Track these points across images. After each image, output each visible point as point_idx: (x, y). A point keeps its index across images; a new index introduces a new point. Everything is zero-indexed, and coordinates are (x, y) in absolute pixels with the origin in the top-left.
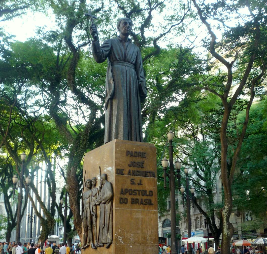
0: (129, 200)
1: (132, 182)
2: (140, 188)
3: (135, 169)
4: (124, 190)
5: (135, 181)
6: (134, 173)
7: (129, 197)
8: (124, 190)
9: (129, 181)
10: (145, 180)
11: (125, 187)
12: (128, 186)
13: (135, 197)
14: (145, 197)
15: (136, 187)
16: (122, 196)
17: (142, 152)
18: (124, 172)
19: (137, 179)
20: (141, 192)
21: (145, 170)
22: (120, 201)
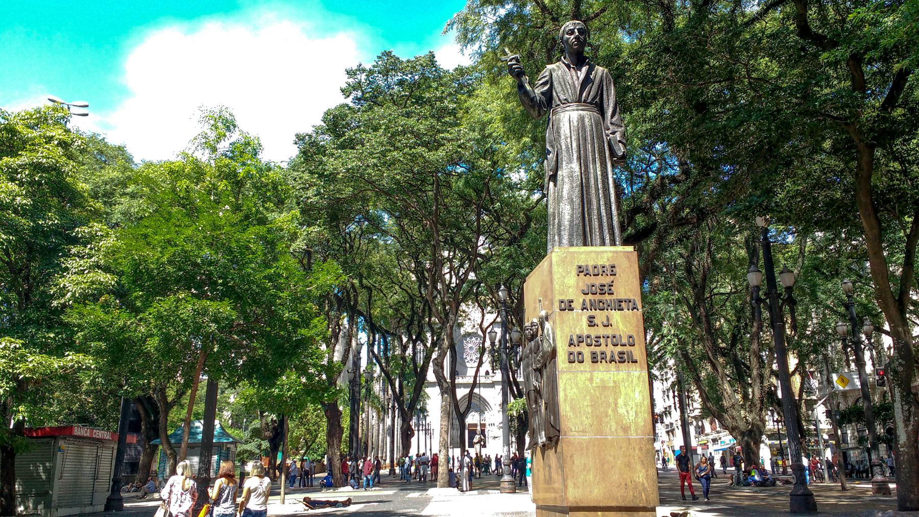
1: (591, 322)
2: (609, 332)
3: (598, 297)
4: (575, 338)
5: (596, 321)
6: (593, 306)
7: (586, 351)
8: (575, 338)
9: (584, 321)
10: (616, 316)
11: (578, 332)
13: (598, 350)
14: (619, 349)
15: (601, 331)
16: (575, 350)
17: (607, 264)
18: (573, 305)
20: (609, 340)
21: (614, 297)
22: (569, 358)
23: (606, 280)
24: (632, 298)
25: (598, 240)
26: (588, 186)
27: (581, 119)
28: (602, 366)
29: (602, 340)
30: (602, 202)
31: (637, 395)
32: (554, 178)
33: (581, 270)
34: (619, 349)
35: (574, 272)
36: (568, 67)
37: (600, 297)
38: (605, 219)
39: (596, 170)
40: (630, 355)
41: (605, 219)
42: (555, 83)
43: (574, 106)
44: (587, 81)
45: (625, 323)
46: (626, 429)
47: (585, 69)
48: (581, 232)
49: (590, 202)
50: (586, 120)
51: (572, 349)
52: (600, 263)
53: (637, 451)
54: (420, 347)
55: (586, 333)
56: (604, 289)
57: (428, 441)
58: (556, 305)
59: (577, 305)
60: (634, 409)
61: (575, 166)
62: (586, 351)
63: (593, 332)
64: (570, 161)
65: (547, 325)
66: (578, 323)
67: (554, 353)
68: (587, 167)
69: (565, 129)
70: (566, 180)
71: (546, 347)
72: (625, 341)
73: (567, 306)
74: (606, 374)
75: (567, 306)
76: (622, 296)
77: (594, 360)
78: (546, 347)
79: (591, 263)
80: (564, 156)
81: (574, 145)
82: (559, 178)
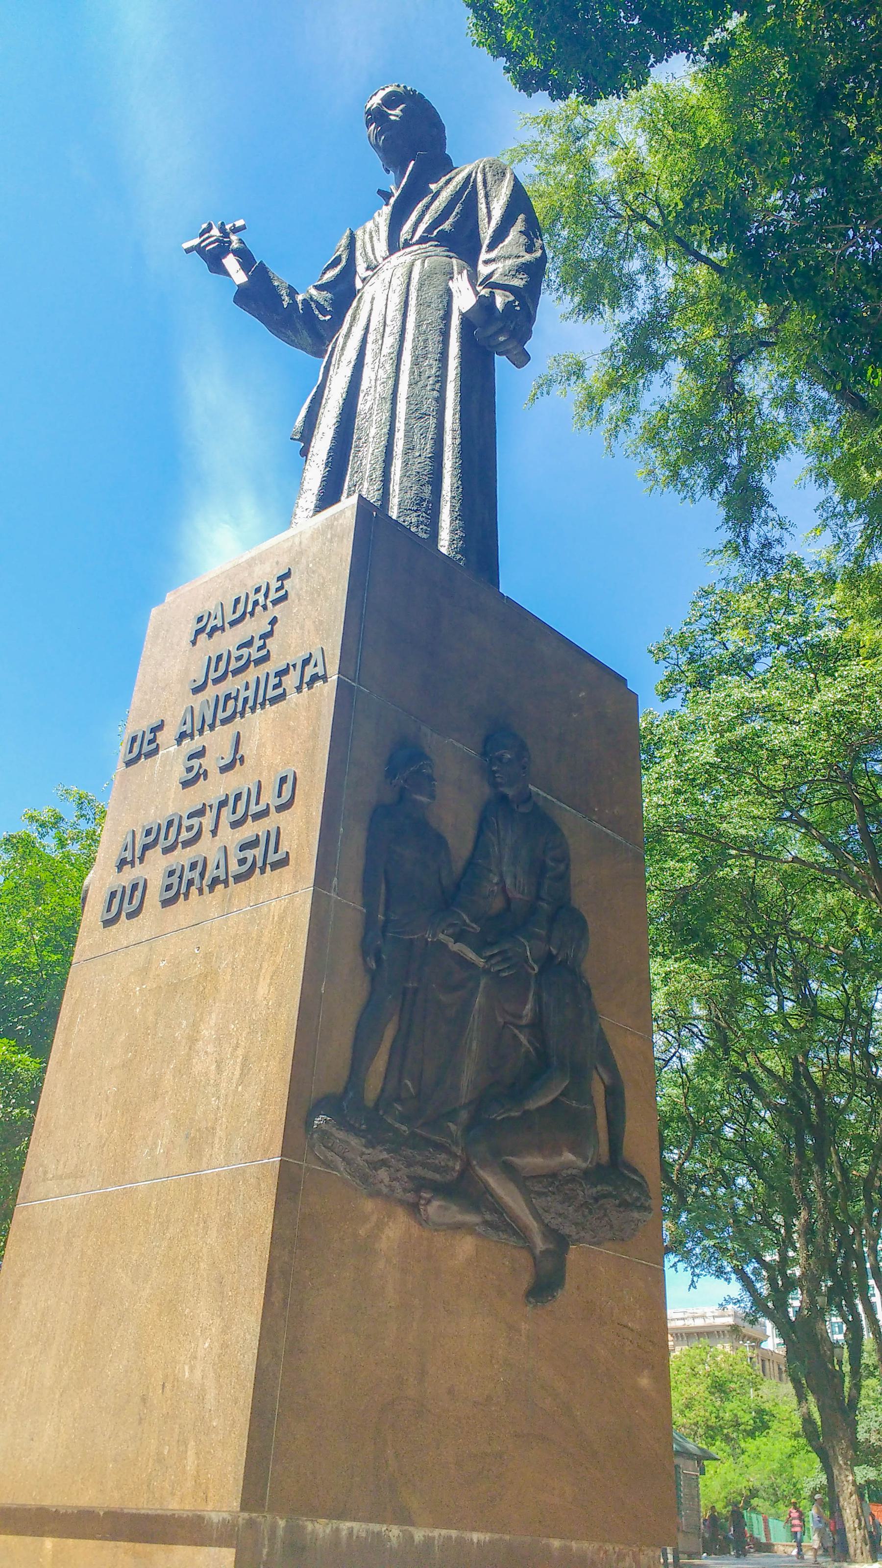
31: (262, 989)
53: (214, 1233)
60: (240, 1052)
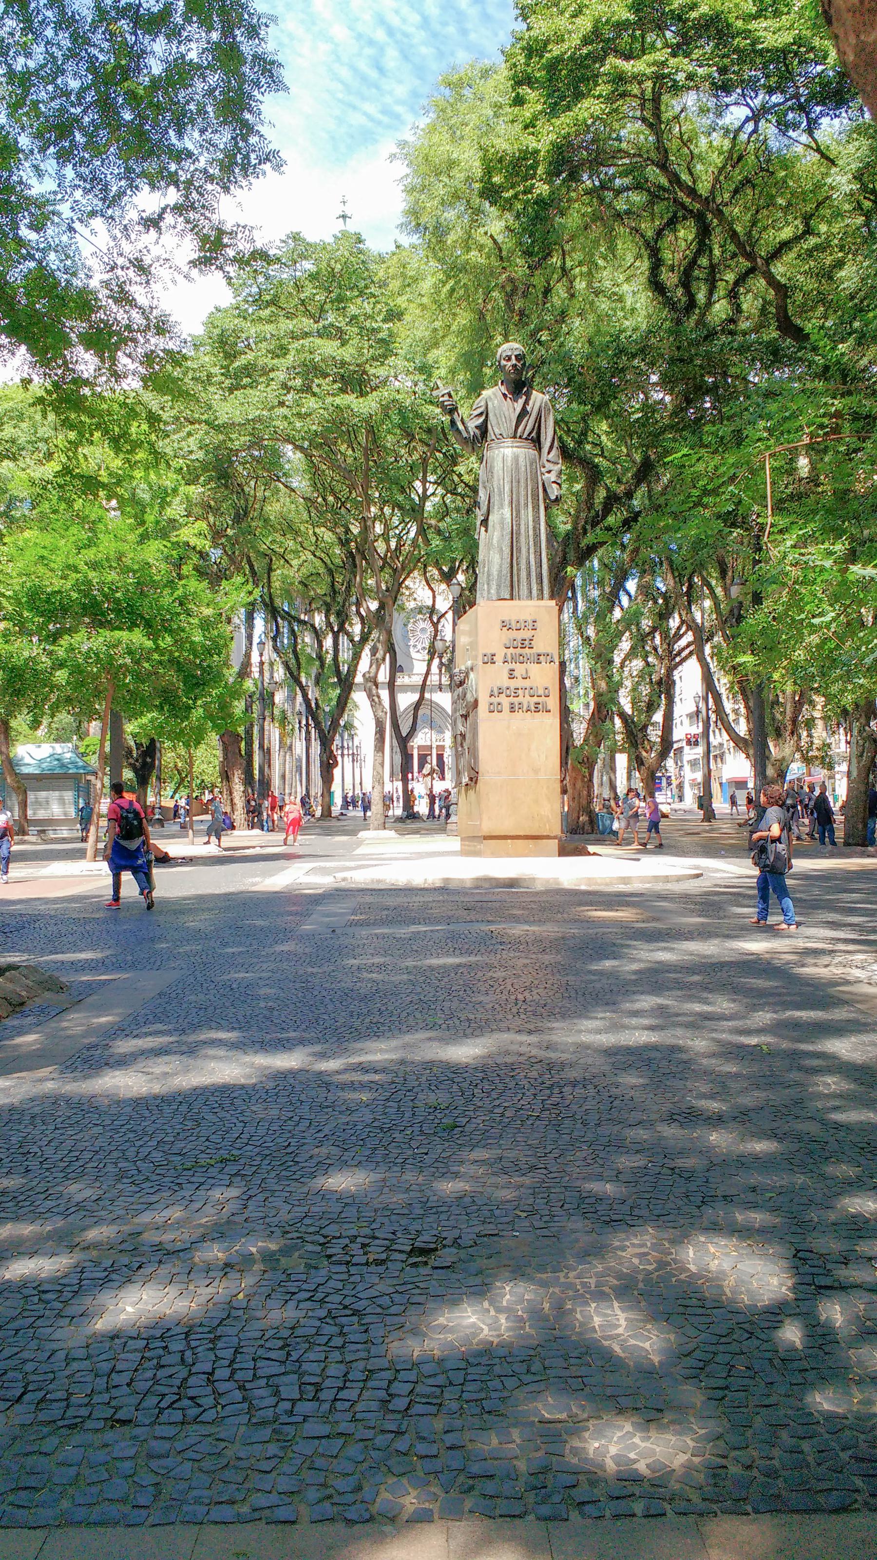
0: (506, 707)
1: (511, 677)
2: (527, 683)
3: (519, 651)
5: (515, 674)
7: (505, 702)
9: (506, 675)
10: (534, 668)
11: (499, 685)
12: (505, 682)
13: (516, 701)
14: (536, 699)
15: (519, 683)
16: (495, 700)
19: (520, 669)
23: (526, 634)
24: (549, 651)
25: (524, 591)
26: (518, 534)
27: (516, 458)
28: (519, 715)
29: (520, 692)
30: (532, 550)
32: (485, 522)
33: (504, 625)
34: (536, 699)
35: (499, 625)
36: (505, 395)
37: (521, 650)
38: (533, 568)
39: (528, 515)
40: (545, 705)
41: (533, 568)
42: (491, 415)
43: (509, 442)
44: (524, 413)
45: (544, 676)
46: (536, 771)
47: (521, 401)
48: (508, 583)
49: (519, 550)
50: (521, 460)
51: (493, 699)
52: (522, 618)
54: (343, 640)
55: (505, 685)
56: (525, 644)
57: (357, 771)
58: (480, 657)
59: (499, 659)
61: (507, 512)
62: (505, 702)
63: (513, 684)
64: (501, 506)
65: (472, 675)
66: (498, 675)
67: (476, 703)
68: (518, 512)
69: (498, 466)
70: (498, 527)
71: (470, 698)
72: (541, 692)
73: (491, 659)
74: (523, 721)
75: (491, 659)
76: (541, 650)
77: (512, 710)
78: (470, 698)
79: (514, 618)
80: (496, 499)
81: (507, 488)
82: (490, 523)
